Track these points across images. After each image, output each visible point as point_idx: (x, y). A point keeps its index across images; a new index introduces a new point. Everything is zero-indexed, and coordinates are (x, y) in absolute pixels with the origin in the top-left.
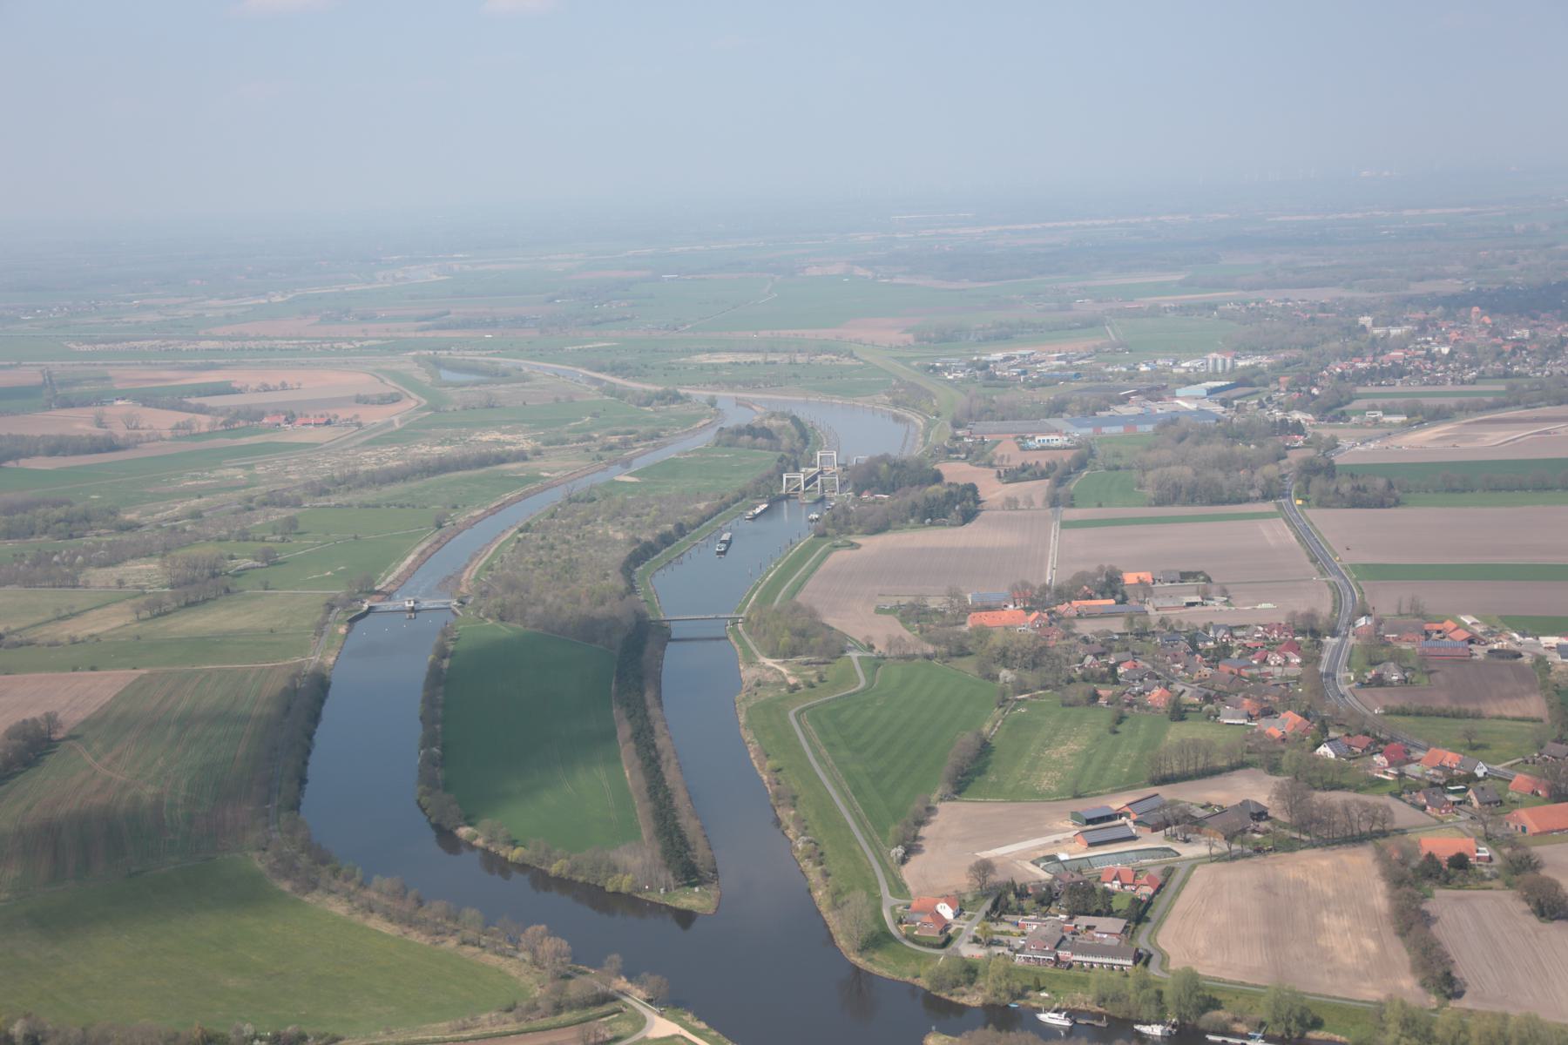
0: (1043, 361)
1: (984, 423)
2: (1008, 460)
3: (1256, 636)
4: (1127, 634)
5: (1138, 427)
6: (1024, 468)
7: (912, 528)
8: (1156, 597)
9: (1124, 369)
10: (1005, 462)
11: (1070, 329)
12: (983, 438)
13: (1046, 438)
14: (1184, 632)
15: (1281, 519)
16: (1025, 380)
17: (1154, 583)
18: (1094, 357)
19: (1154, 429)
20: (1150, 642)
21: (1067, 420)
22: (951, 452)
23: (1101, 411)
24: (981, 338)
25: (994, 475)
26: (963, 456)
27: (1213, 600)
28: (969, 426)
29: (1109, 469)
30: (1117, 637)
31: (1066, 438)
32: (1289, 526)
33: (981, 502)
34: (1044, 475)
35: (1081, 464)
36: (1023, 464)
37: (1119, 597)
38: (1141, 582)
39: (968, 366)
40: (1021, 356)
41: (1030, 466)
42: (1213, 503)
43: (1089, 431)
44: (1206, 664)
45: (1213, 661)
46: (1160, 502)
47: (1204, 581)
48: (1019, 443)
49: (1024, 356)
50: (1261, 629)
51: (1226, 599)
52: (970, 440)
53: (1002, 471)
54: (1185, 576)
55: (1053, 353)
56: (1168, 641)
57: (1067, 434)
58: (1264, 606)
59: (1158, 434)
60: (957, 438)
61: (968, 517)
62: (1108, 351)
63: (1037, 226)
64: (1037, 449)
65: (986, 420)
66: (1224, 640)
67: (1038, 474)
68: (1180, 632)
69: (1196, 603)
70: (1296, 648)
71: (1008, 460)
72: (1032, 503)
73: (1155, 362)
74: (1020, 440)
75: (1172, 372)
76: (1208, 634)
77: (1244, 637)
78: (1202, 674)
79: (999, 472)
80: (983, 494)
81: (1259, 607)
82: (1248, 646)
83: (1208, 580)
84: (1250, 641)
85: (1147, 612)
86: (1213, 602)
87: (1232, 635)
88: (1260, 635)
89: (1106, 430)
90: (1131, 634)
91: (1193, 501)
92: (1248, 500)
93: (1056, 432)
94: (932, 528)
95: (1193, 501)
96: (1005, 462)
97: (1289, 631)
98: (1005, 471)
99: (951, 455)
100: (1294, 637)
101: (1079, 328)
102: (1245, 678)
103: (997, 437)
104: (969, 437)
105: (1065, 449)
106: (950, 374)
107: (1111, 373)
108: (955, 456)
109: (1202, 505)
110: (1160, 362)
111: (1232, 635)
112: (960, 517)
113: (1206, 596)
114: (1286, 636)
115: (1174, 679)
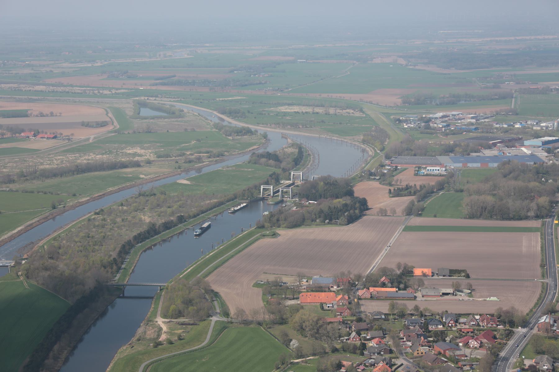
0: (464, 119)
1: (402, 157)
2: (401, 183)
3: (472, 323)
4: (390, 315)
5: (489, 164)
6: (408, 188)
7: (317, 225)
8: (426, 288)
9: (505, 126)
10: (398, 183)
11: (492, 99)
12: (396, 167)
13: (432, 168)
14: (429, 316)
15: (539, 233)
16: (445, 130)
17: (432, 276)
18: (494, 118)
19: (498, 166)
20: (402, 321)
21: (450, 158)
22: (371, 174)
23: (475, 152)
24: (438, 103)
25: (388, 191)
26: (378, 178)
27: (462, 292)
28: (393, 159)
29: (457, 191)
30: (383, 317)
31: (444, 169)
32: (541, 238)
33: (368, 209)
34: (415, 194)
35: (441, 186)
36: (407, 185)
37: (402, 286)
38: (424, 275)
39: (419, 120)
40: (453, 115)
41: (411, 187)
42: (503, 219)
43: (459, 165)
44: (426, 343)
45: (434, 341)
46: (472, 216)
47: (464, 276)
48: (415, 171)
49: (455, 115)
50: (477, 317)
51: (470, 291)
52: (389, 168)
53: (392, 188)
54: (453, 272)
55: (472, 114)
56: (412, 323)
57: (446, 166)
58: (493, 298)
59: (499, 169)
60: (382, 166)
61: (351, 220)
62: (503, 115)
63: (513, 38)
64: (424, 175)
65: (404, 155)
66: (450, 325)
67: (412, 191)
68: (426, 316)
69: (449, 293)
70: (491, 335)
71: (401, 183)
72: (394, 212)
73: (526, 122)
74: (417, 169)
75: (532, 129)
76: (442, 318)
77: (465, 324)
78: (420, 352)
79: (390, 190)
80: (370, 204)
81: (488, 299)
82: (463, 331)
83: (468, 276)
84: (467, 327)
85: (415, 297)
86: (460, 293)
87: (456, 321)
88: (474, 323)
89: (470, 165)
90: (394, 314)
91: (491, 217)
92: (527, 218)
93: (441, 165)
94: (329, 225)
95: (491, 217)
96: (398, 183)
97: (494, 322)
98: (394, 189)
99: (371, 177)
100: (497, 325)
101: (496, 99)
102: (446, 357)
103: (405, 166)
104: (389, 165)
105: (440, 176)
106: (406, 125)
107: (497, 128)
108: (373, 177)
109: (497, 219)
110: (529, 122)
111: (456, 321)
112: (346, 220)
113: (458, 289)
114: (492, 325)
115: (402, 354)
